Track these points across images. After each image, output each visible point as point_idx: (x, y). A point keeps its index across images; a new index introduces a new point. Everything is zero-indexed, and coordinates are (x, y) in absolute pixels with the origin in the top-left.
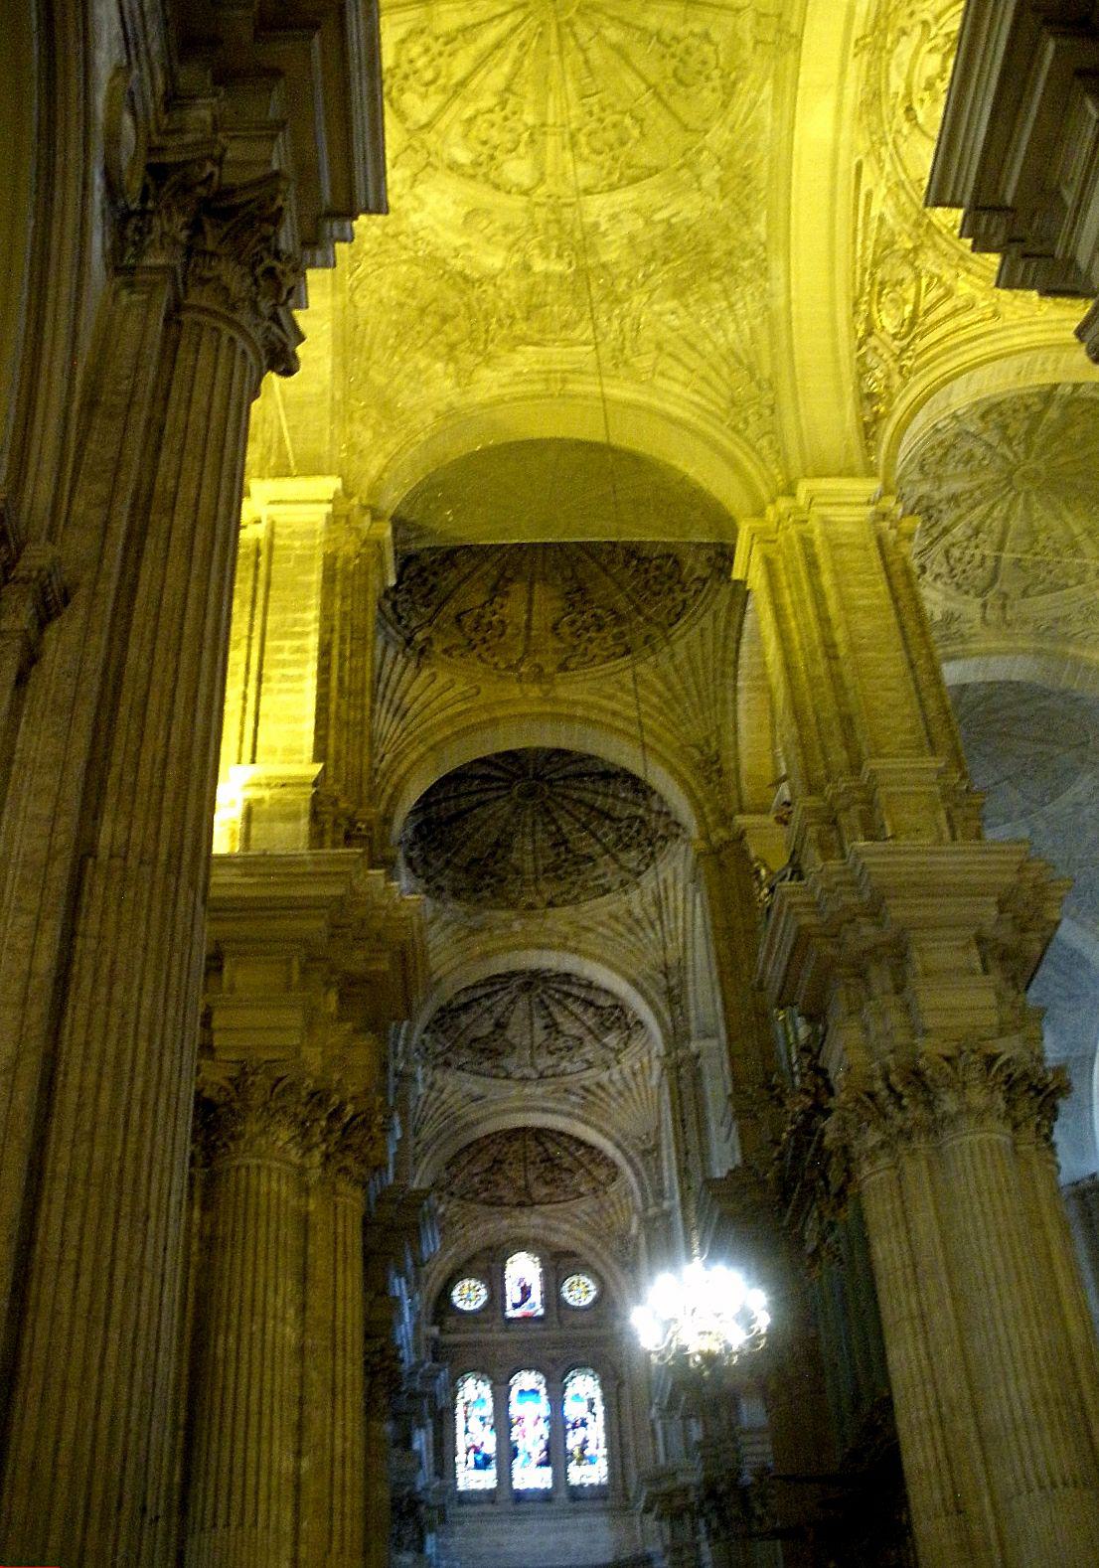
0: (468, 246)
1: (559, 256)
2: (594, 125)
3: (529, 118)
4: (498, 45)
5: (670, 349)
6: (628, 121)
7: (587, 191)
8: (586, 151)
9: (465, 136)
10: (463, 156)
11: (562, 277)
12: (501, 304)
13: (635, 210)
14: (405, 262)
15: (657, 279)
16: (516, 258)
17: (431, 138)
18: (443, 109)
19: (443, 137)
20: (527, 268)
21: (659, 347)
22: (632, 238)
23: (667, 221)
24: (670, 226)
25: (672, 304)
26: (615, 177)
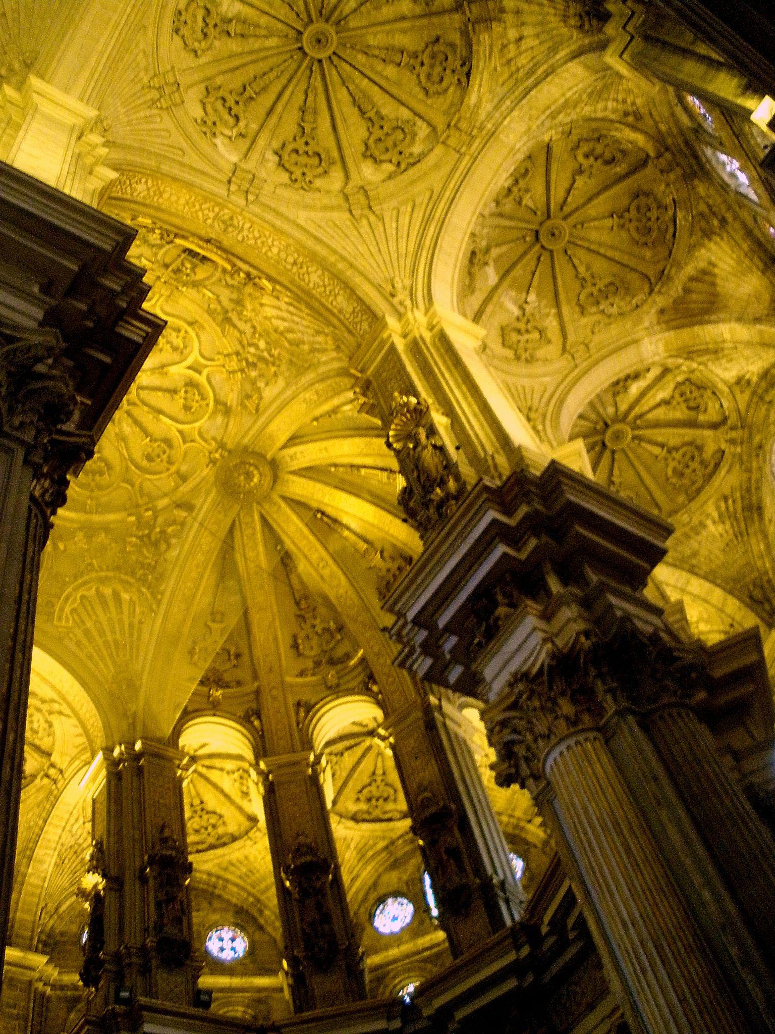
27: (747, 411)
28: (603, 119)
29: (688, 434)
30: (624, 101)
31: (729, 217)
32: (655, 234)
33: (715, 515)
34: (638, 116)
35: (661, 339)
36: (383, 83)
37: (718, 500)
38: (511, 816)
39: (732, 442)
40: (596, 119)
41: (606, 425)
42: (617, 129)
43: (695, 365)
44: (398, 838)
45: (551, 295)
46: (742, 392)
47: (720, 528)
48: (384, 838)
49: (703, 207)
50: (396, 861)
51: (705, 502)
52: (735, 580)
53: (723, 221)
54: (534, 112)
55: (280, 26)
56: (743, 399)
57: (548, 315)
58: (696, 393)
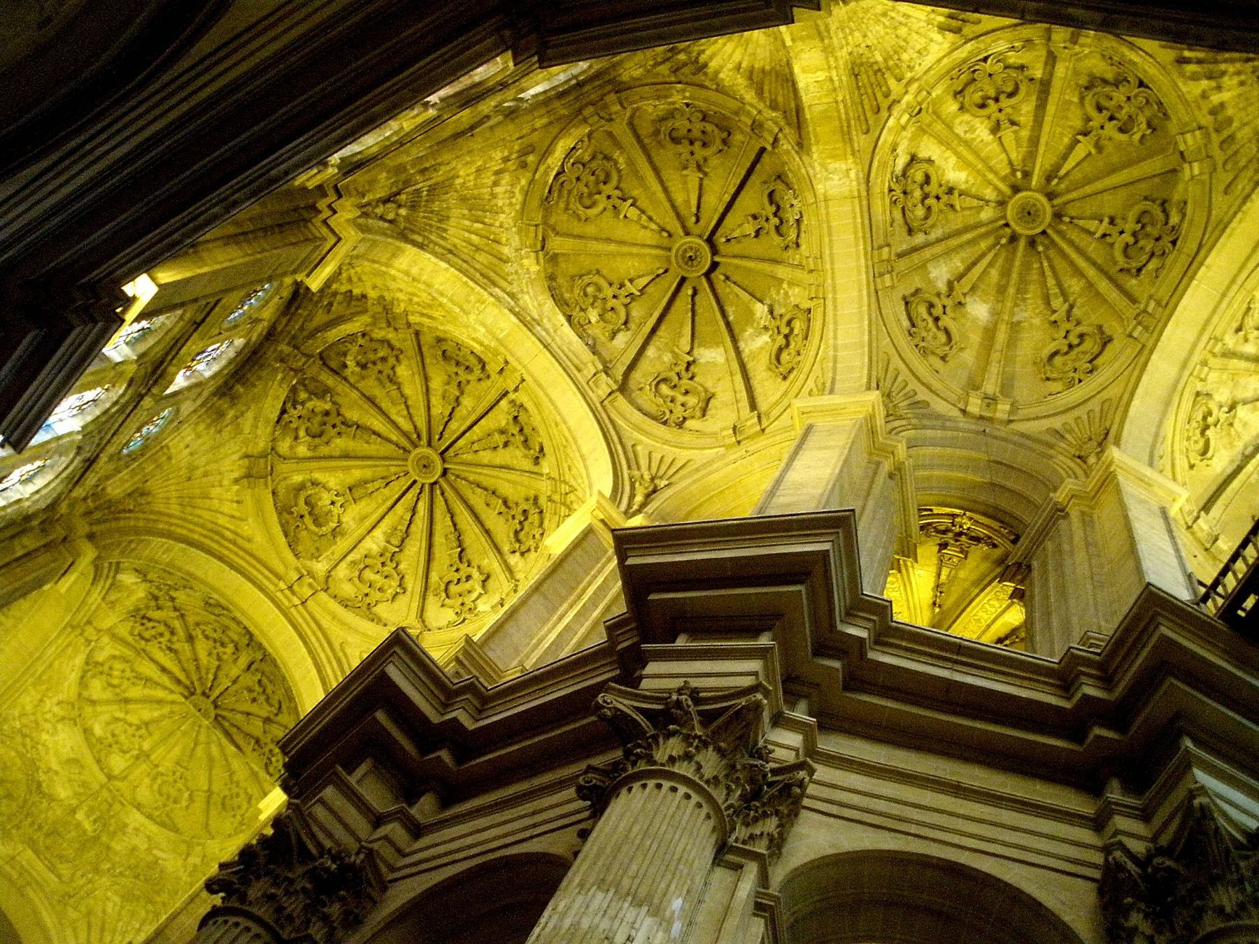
0: (56, 773)
1: (95, 821)
2: (171, 779)
3: (146, 746)
4: (159, 702)
5: (93, 920)
6: (186, 795)
7: (138, 807)
8: (156, 787)
9: (108, 724)
10: (98, 730)
11: (85, 832)
12: (43, 816)
13: (149, 838)
14: (17, 752)
15: (123, 881)
16: (74, 802)
17: (88, 710)
18: (107, 702)
19: (96, 715)
20: (73, 811)
21: (89, 914)
22: (134, 849)
23: (157, 859)
24: (156, 862)
25: (117, 899)
26: (156, 813)
30: (498, 173)
32: (709, 128)
33: (1205, 83)
36: (473, 418)
37: (1182, 75)
40: (524, 203)
42: (546, 173)
51: (1181, 97)
54: (472, 298)
55: (409, 495)
57: (786, 293)
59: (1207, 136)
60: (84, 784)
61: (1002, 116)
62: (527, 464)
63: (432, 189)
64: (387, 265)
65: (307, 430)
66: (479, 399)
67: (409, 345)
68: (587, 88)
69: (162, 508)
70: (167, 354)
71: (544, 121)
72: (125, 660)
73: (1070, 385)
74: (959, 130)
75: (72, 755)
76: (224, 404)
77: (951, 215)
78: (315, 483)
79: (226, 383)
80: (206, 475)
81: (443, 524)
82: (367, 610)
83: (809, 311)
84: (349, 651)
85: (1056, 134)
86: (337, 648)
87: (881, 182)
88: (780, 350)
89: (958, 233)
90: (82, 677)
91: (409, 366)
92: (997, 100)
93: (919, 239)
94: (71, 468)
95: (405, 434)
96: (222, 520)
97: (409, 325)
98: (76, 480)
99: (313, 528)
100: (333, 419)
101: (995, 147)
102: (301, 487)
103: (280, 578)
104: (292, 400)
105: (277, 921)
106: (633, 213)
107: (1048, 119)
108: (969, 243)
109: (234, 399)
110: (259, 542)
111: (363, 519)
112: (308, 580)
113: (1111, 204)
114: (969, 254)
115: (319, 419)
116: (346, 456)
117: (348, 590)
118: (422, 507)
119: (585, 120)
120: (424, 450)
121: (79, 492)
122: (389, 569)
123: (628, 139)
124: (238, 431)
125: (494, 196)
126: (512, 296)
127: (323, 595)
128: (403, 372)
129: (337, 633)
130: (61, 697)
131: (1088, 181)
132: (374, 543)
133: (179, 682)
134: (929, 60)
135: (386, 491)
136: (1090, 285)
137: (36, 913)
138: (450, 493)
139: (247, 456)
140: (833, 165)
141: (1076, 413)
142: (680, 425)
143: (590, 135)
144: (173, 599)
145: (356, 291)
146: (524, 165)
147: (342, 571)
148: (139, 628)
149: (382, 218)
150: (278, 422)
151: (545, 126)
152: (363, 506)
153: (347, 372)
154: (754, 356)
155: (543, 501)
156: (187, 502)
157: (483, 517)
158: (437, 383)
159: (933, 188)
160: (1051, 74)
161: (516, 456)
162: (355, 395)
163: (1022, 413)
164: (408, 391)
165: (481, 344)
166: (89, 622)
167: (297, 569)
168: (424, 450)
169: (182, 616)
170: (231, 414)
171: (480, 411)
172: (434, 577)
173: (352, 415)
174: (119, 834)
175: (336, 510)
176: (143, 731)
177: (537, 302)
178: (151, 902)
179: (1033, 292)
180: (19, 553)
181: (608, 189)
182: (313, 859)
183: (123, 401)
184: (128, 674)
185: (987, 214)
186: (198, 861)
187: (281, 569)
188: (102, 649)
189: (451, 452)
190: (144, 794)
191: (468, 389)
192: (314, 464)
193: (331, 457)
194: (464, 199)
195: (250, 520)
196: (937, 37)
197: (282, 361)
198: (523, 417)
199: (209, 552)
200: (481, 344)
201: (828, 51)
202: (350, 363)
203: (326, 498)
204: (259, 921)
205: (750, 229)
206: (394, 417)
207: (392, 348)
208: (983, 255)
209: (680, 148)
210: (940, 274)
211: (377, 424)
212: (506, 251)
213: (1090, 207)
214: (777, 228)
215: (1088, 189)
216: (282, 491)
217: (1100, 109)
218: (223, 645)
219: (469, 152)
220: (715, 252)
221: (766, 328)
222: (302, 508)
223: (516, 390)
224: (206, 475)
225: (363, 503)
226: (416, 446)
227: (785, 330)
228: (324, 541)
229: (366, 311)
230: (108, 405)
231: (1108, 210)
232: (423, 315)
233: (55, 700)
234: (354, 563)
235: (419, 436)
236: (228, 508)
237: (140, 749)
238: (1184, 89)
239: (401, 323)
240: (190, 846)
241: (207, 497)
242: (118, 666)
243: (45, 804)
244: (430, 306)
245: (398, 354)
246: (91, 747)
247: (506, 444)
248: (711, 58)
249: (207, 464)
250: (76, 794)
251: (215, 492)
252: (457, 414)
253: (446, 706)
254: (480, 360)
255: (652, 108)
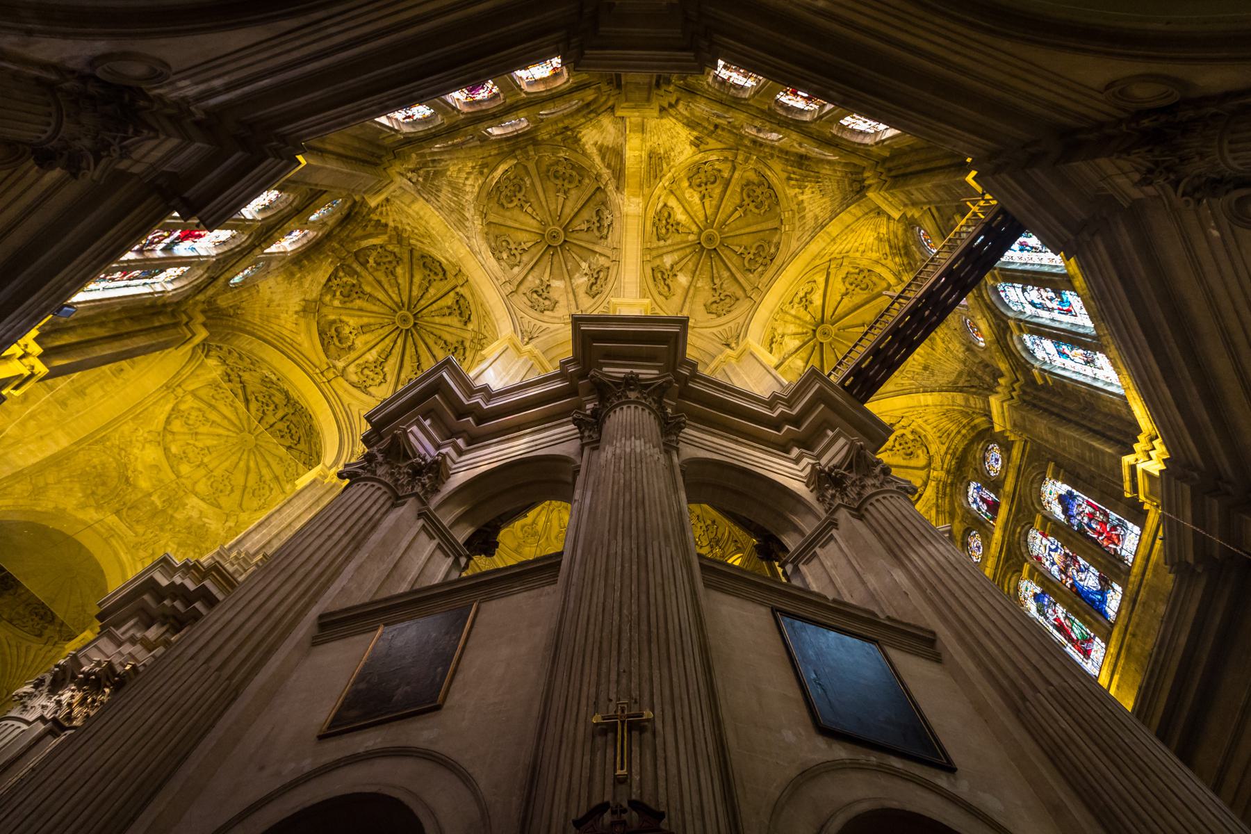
0: (141, 473)
1: (164, 501)
6: (229, 488)
7: (196, 494)
8: (209, 483)
10: (174, 449)
11: (156, 507)
14: (114, 458)
15: (181, 535)
16: (151, 490)
17: (169, 437)
18: (184, 434)
19: (174, 440)
20: (150, 495)
22: (190, 518)
24: (204, 525)
27: (725, 143)
28: (481, 188)
29: (734, 187)
30: (469, 173)
31: (561, 125)
32: (574, 173)
34: (484, 165)
35: (628, 198)
36: (435, 298)
37: (788, 185)
38: (964, 427)
39: (746, 160)
40: (479, 193)
41: (700, 243)
42: (492, 180)
43: (669, 175)
44: (937, 500)
45: (590, 253)
46: (707, 144)
47: (808, 191)
48: (930, 508)
49: (559, 138)
50: (950, 514)
51: (786, 195)
52: (844, 199)
53: (566, 128)
54: (448, 235)
55: (393, 334)
56: (712, 143)
58: (702, 175)
59: (794, 214)
60: (161, 481)
61: (706, 193)
62: (459, 325)
63: (436, 173)
64: (409, 206)
65: (341, 292)
66: (438, 290)
67: (406, 256)
68: (520, 139)
69: (249, 318)
70: (276, 225)
71: (496, 152)
72: (200, 410)
73: (719, 316)
74: (687, 196)
75: (153, 463)
76: (295, 269)
77: (676, 235)
78: (341, 321)
79: (298, 257)
80: (279, 305)
81: (410, 350)
82: (364, 389)
83: (608, 268)
84: (352, 408)
85: (728, 205)
86: (346, 406)
87: (651, 213)
88: (593, 284)
89: (678, 244)
90: (168, 418)
91: (403, 268)
92: (706, 184)
93: (662, 243)
94: (200, 280)
95: (396, 304)
96: (285, 332)
97: (410, 245)
98: (199, 289)
99: (337, 344)
100: (357, 289)
101: (701, 206)
102: (334, 322)
103: (316, 367)
104: (334, 275)
105: (396, 485)
106: (530, 210)
107: (726, 197)
108: (682, 249)
109: (301, 268)
110: (306, 345)
111: (367, 343)
112: (332, 370)
113: (746, 240)
114: (681, 253)
115: (348, 288)
116: (361, 310)
117: (354, 378)
118: (400, 342)
119: (516, 157)
120: (404, 312)
121: (200, 297)
122: (378, 370)
123: (533, 172)
124: (301, 284)
125: (464, 185)
126: (468, 238)
127: (340, 379)
128: (399, 270)
129: (346, 399)
130: (153, 428)
131: (738, 229)
132: (372, 356)
133: (235, 425)
134: (682, 158)
135: (381, 331)
136: (732, 275)
137: (116, 554)
138: (416, 335)
139: (304, 300)
140: (633, 199)
141: (723, 327)
142: (542, 312)
143: (515, 165)
144: (240, 377)
145: (383, 221)
146: (481, 173)
147: (352, 368)
148: (213, 392)
149: (410, 180)
150: (325, 285)
151: (495, 155)
152: (368, 337)
153: (368, 265)
154: (578, 286)
155: (467, 344)
156: (267, 319)
157: (433, 349)
158: (417, 279)
159: (671, 221)
160: (731, 177)
161: (454, 321)
162: (370, 278)
163: (700, 325)
164: (400, 281)
165: (447, 260)
166: (179, 385)
167: (327, 364)
168: (404, 312)
169: (244, 387)
170: (299, 275)
171: (438, 296)
172: (403, 376)
173: (368, 289)
174: (181, 509)
175: (352, 337)
176: (206, 451)
177: (479, 243)
178: (198, 547)
179: (707, 275)
180: (157, 324)
181: (520, 195)
182: (410, 459)
183: (243, 246)
184: (201, 418)
185: (691, 237)
186: (232, 524)
187: (317, 363)
188: (185, 402)
189: (419, 315)
190: (202, 487)
191: (434, 284)
192: (342, 311)
193: (352, 309)
194: (450, 183)
195: (302, 335)
196: (688, 147)
197: (333, 252)
198: (462, 301)
199: (276, 347)
200: (447, 260)
201: (643, 140)
202: (371, 260)
203: (347, 330)
204: (386, 484)
205: (585, 227)
206: (390, 293)
207: (396, 257)
208: (686, 256)
209: (557, 182)
210: (668, 260)
211: (381, 295)
212: (467, 215)
213: (736, 241)
214: (598, 228)
215: (738, 233)
216: (322, 322)
217: (749, 196)
218: (267, 405)
219: (457, 158)
220: (566, 236)
221: (586, 274)
222: (333, 332)
223: (462, 286)
224: (279, 305)
225: (367, 335)
226: (400, 310)
227: (596, 276)
228: (342, 352)
229: (386, 233)
230: (233, 246)
231: (744, 243)
232: (418, 240)
233: (147, 430)
234: (359, 365)
235: (403, 305)
236: (289, 326)
237: (202, 461)
238: (788, 192)
239: (405, 243)
240: (228, 515)
241: (278, 317)
242: (194, 413)
243: (130, 490)
244: (423, 236)
245: (399, 260)
246: (168, 458)
247: (450, 314)
248: (583, 136)
249: (280, 300)
250: (154, 486)
251: (283, 316)
252: (425, 297)
253: (470, 397)
254: (444, 270)
255: (548, 157)
